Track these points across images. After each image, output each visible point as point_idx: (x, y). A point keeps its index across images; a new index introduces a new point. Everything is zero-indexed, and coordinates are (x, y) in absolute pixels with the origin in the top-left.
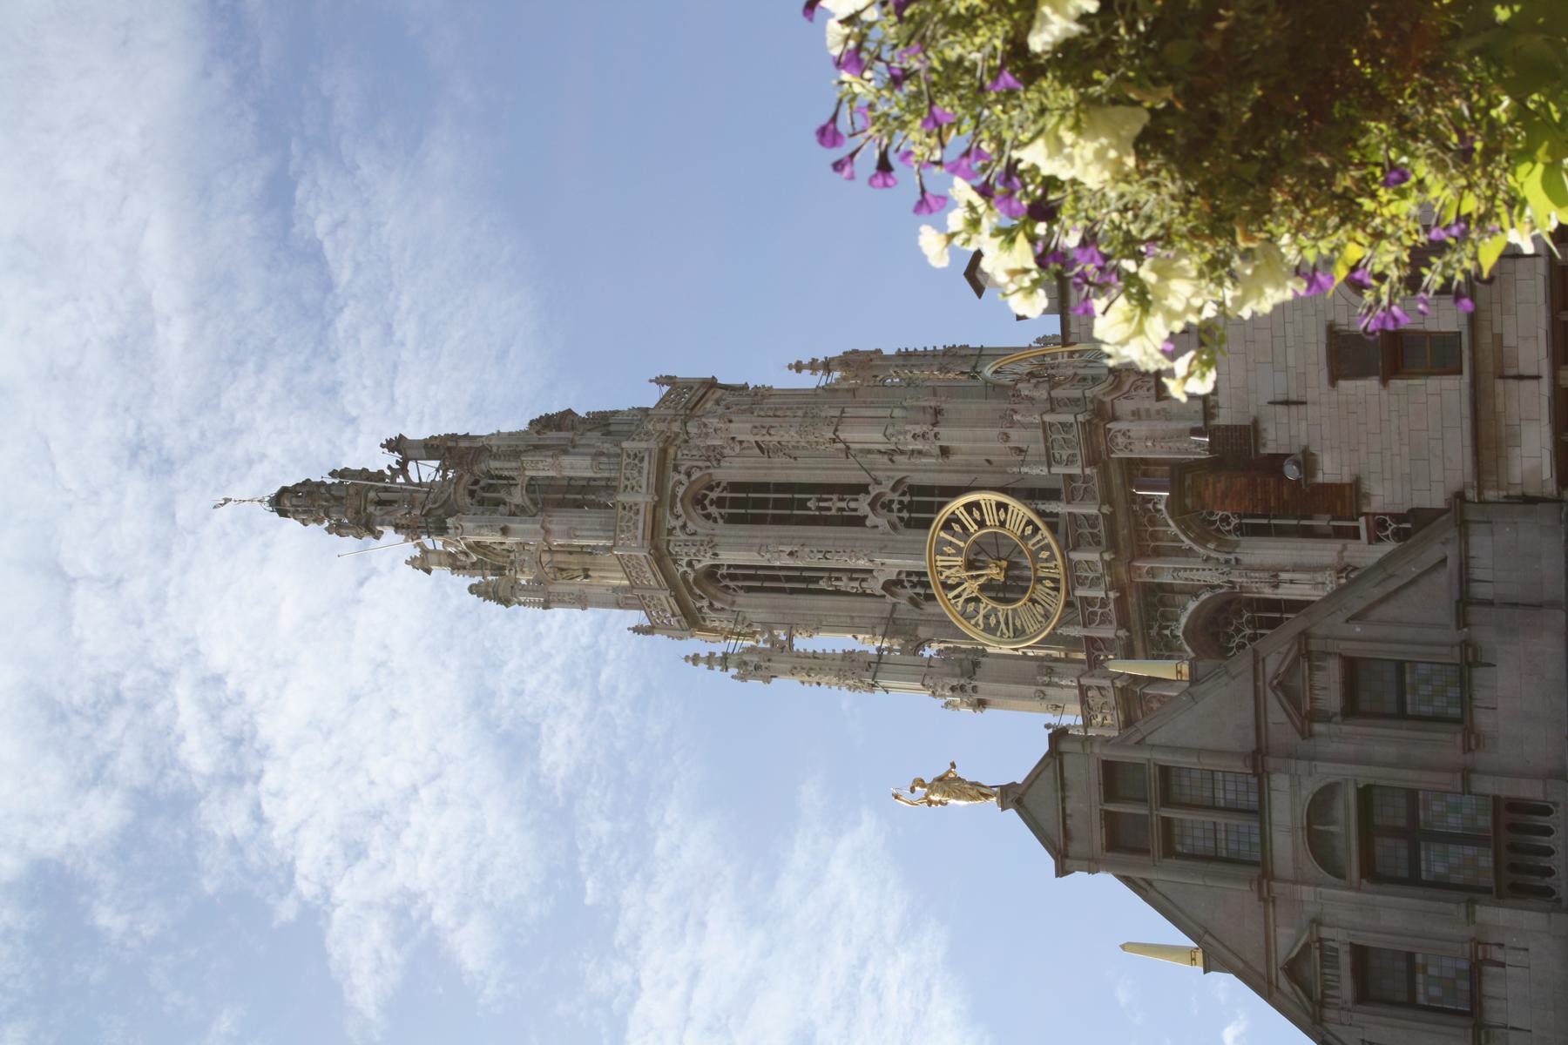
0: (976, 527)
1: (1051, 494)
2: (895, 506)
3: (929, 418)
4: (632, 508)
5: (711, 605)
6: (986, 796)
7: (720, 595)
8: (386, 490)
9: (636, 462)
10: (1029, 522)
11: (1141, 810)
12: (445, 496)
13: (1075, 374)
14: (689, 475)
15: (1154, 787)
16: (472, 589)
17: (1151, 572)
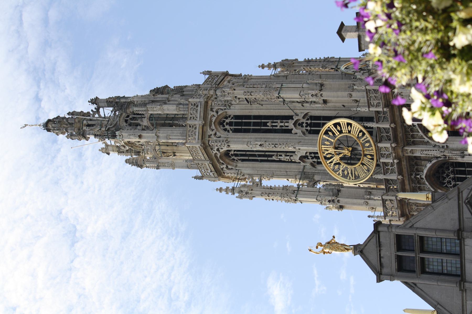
0: (338, 133)
1: (370, 119)
2: (304, 125)
3: (318, 87)
4: (194, 126)
5: (227, 167)
6: (348, 250)
7: (231, 163)
8: (91, 120)
9: (195, 107)
10: (361, 131)
11: (412, 255)
12: (115, 122)
14: (217, 112)
15: (417, 246)
16: (127, 161)
17: (412, 151)
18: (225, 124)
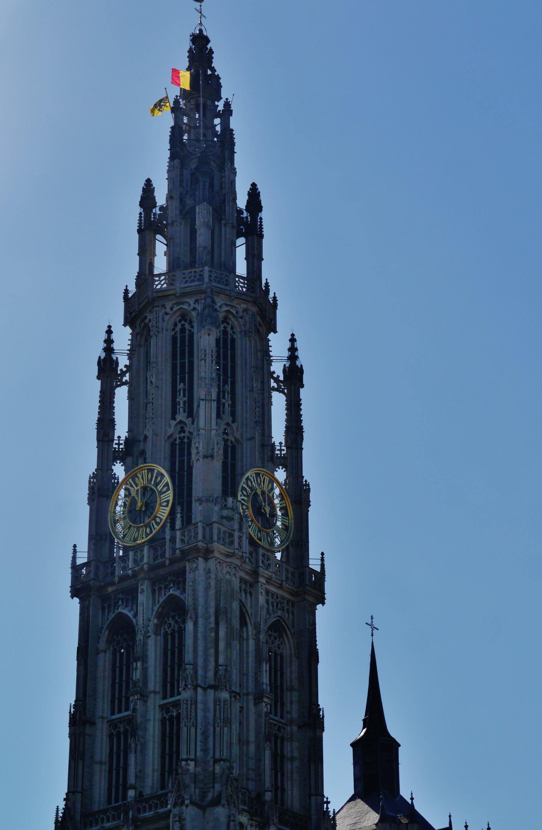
2: (182, 434)
9: (198, 277)
13: (234, 530)
14: (194, 309)
17: (143, 590)
18: (183, 322)
